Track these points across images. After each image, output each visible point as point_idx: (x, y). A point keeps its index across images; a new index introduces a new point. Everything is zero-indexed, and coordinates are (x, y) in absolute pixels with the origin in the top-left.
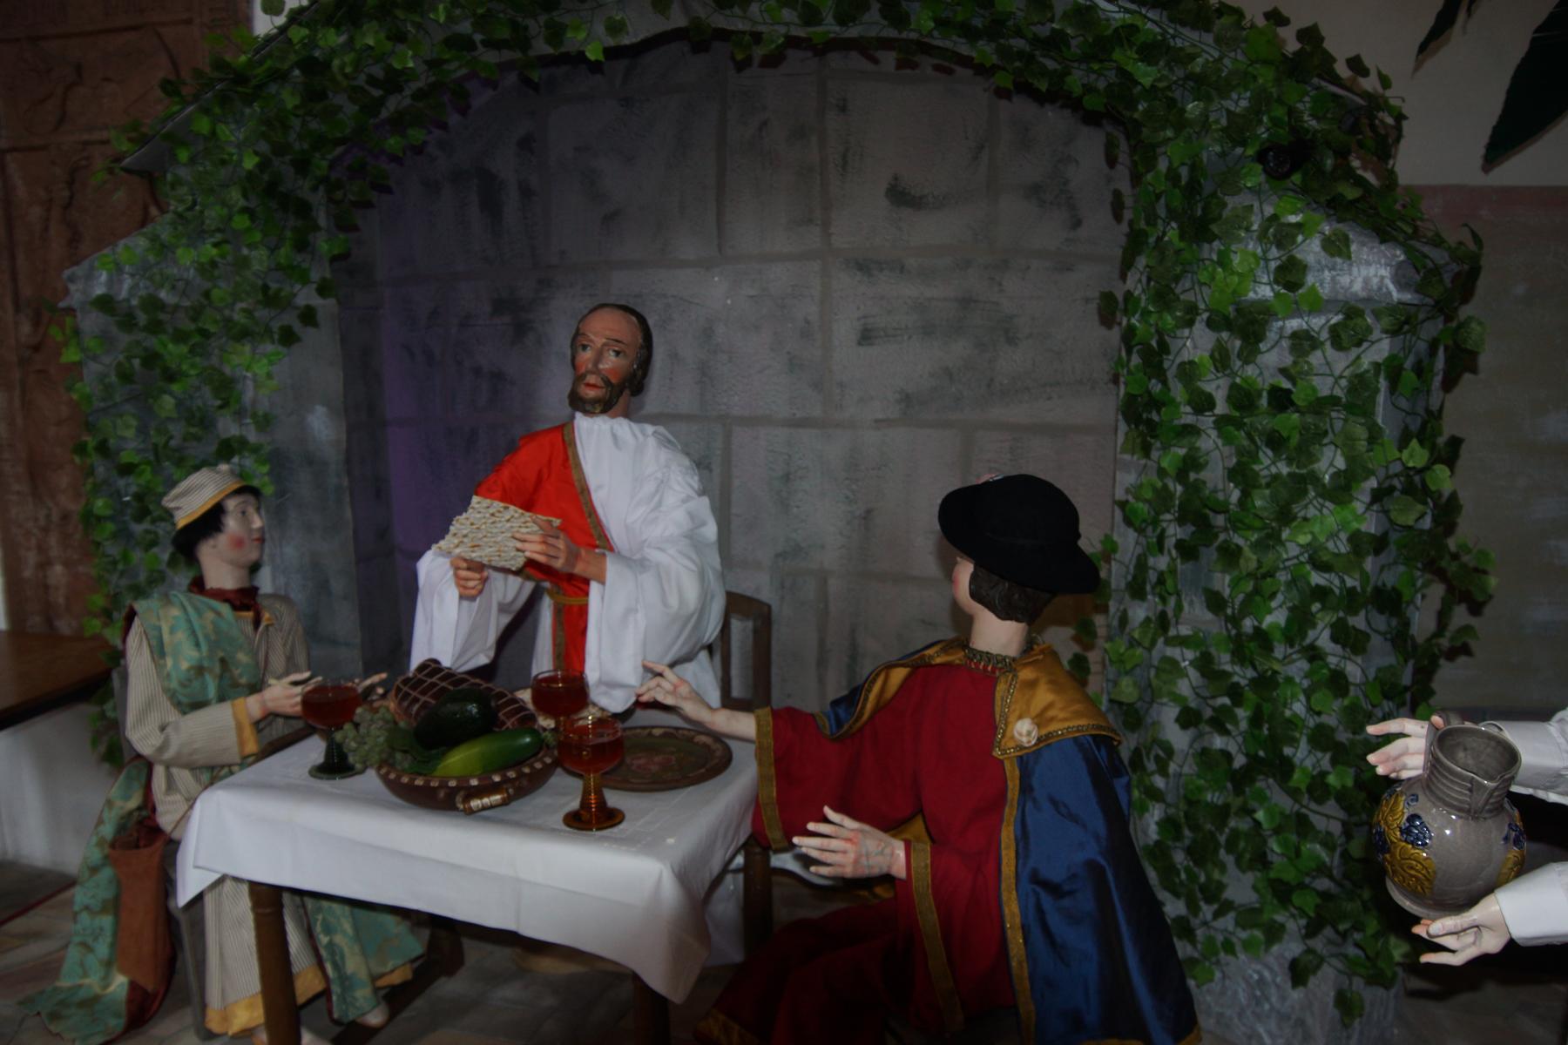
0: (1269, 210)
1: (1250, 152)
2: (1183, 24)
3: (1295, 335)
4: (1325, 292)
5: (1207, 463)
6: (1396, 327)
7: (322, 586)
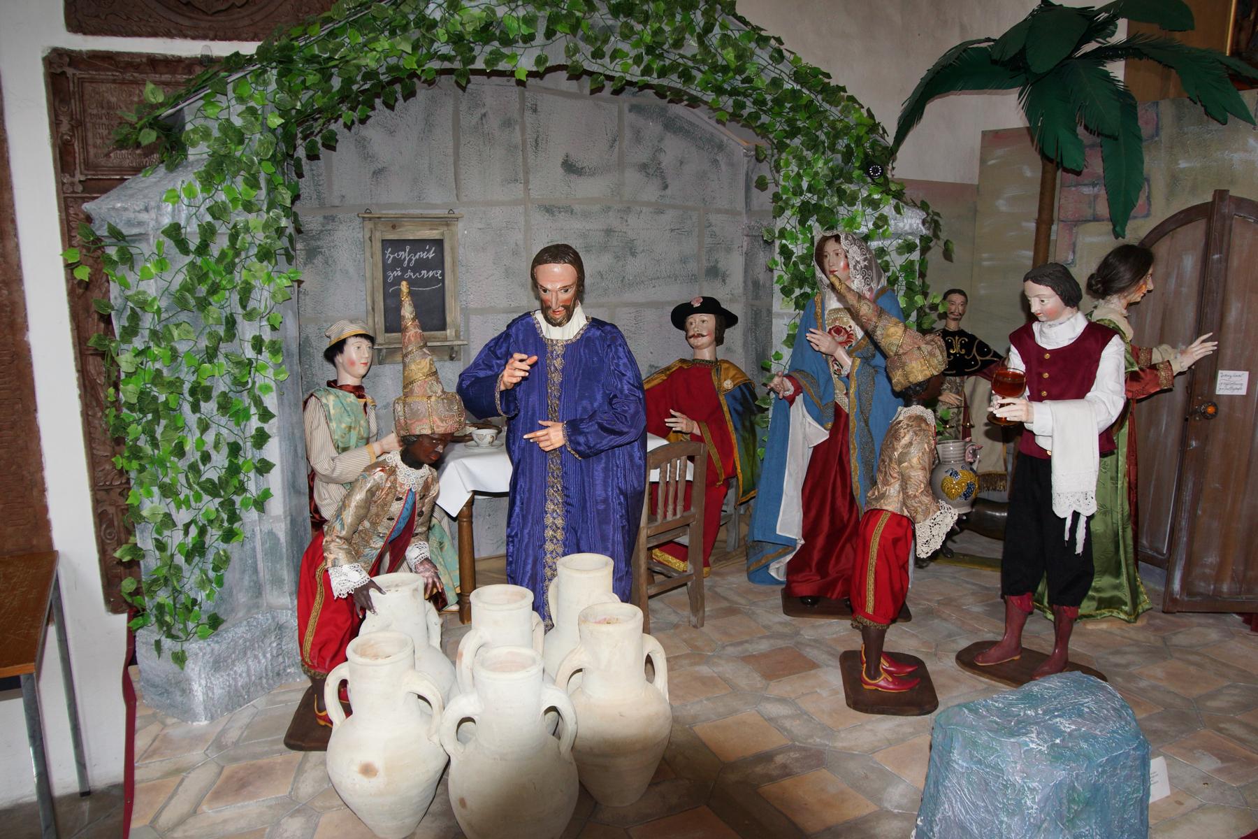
2: (827, 102)
7: (296, 450)
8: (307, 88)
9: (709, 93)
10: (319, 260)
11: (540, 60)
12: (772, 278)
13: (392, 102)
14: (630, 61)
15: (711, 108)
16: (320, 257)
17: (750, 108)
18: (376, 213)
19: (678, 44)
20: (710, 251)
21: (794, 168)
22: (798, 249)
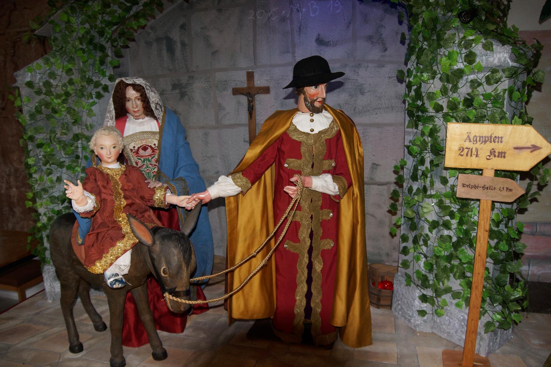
0: (461, 35)
1: (455, 14)
3: (472, 81)
4: (484, 64)
5: (440, 130)
6: (510, 76)
16: (186, 97)
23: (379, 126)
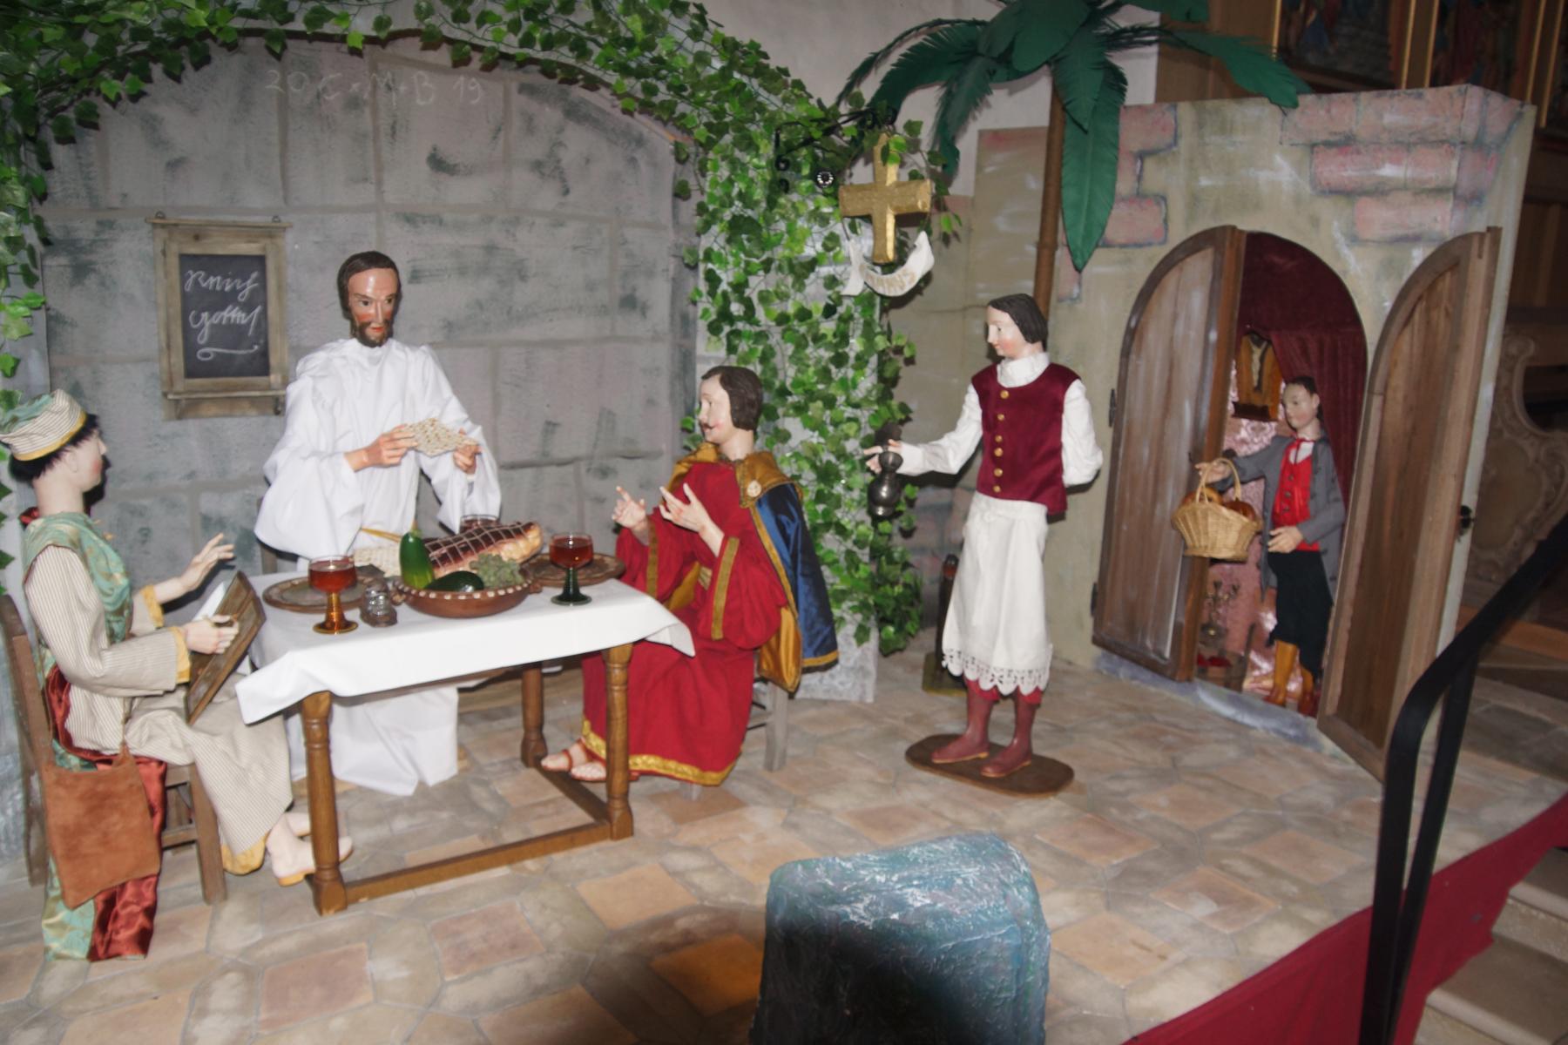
0: (812, 207)
2: (765, 89)
3: (825, 278)
8: (47, 46)
9: (611, 72)
10: (91, 281)
11: (381, 23)
12: (696, 312)
13: (176, 72)
14: (504, 28)
15: (614, 94)
17: (663, 94)
18: (172, 218)
19: (567, 6)
20: (626, 275)
21: (724, 172)
22: (727, 277)
23: (556, 344)
